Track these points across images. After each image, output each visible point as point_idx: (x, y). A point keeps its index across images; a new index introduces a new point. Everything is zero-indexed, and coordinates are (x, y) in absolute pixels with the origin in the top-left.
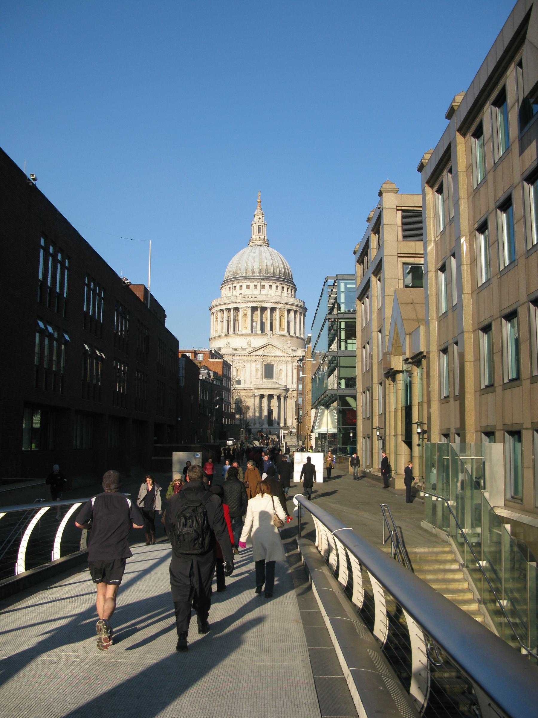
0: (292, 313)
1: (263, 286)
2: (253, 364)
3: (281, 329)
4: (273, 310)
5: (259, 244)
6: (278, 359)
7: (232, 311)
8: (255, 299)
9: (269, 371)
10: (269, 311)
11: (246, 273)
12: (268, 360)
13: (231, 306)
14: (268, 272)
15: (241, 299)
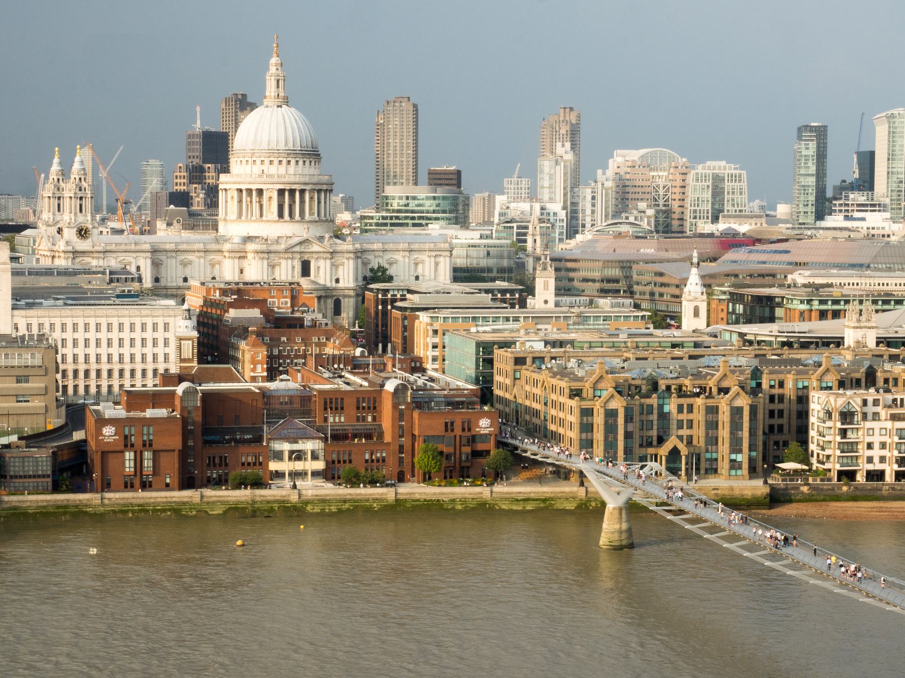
0: (323, 194)
1: (289, 162)
2: (290, 261)
3: (311, 214)
4: (302, 192)
5: (279, 104)
6: (315, 256)
7: (254, 193)
8: (283, 180)
9: (306, 270)
10: (297, 194)
11: (269, 145)
12: (306, 257)
13: (254, 187)
14: (294, 146)
15: (264, 179)
